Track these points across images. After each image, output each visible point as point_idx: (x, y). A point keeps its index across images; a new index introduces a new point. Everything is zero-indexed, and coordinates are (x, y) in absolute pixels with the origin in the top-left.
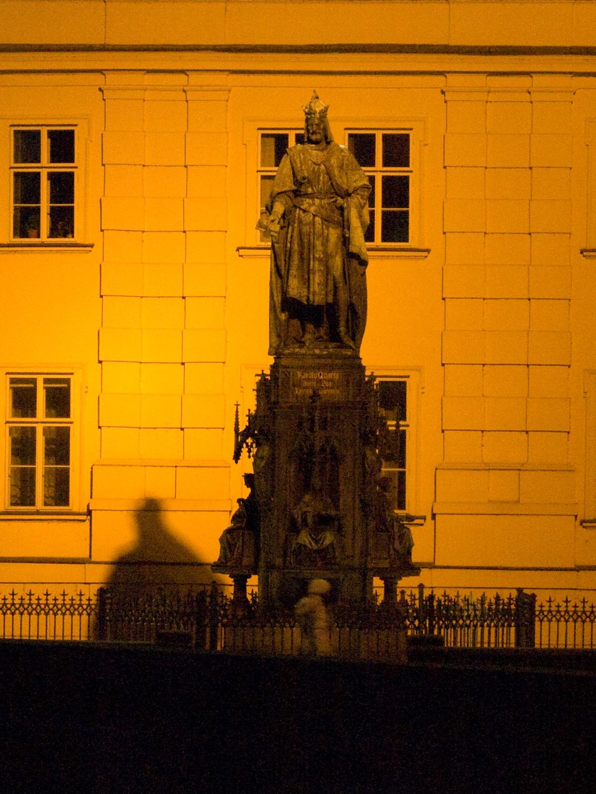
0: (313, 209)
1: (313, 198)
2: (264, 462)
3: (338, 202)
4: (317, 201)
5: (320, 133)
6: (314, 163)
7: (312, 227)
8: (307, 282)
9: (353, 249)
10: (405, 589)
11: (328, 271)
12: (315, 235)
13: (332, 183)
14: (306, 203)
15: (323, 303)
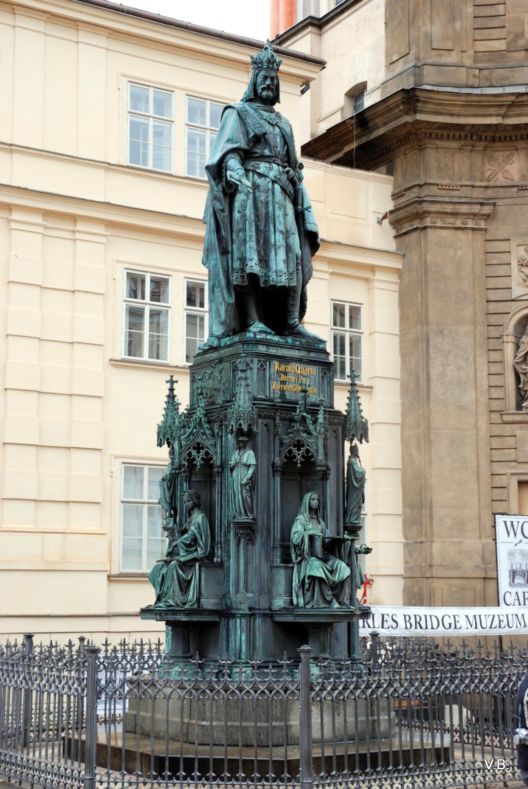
0: (272, 174)
1: (269, 162)
2: (251, 471)
3: (290, 173)
4: (275, 166)
5: (272, 90)
6: (269, 122)
7: (271, 194)
8: (264, 261)
9: (310, 227)
10: (85, 635)
11: (288, 248)
12: (277, 205)
13: (288, 150)
14: (263, 167)
15: (287, 285)
